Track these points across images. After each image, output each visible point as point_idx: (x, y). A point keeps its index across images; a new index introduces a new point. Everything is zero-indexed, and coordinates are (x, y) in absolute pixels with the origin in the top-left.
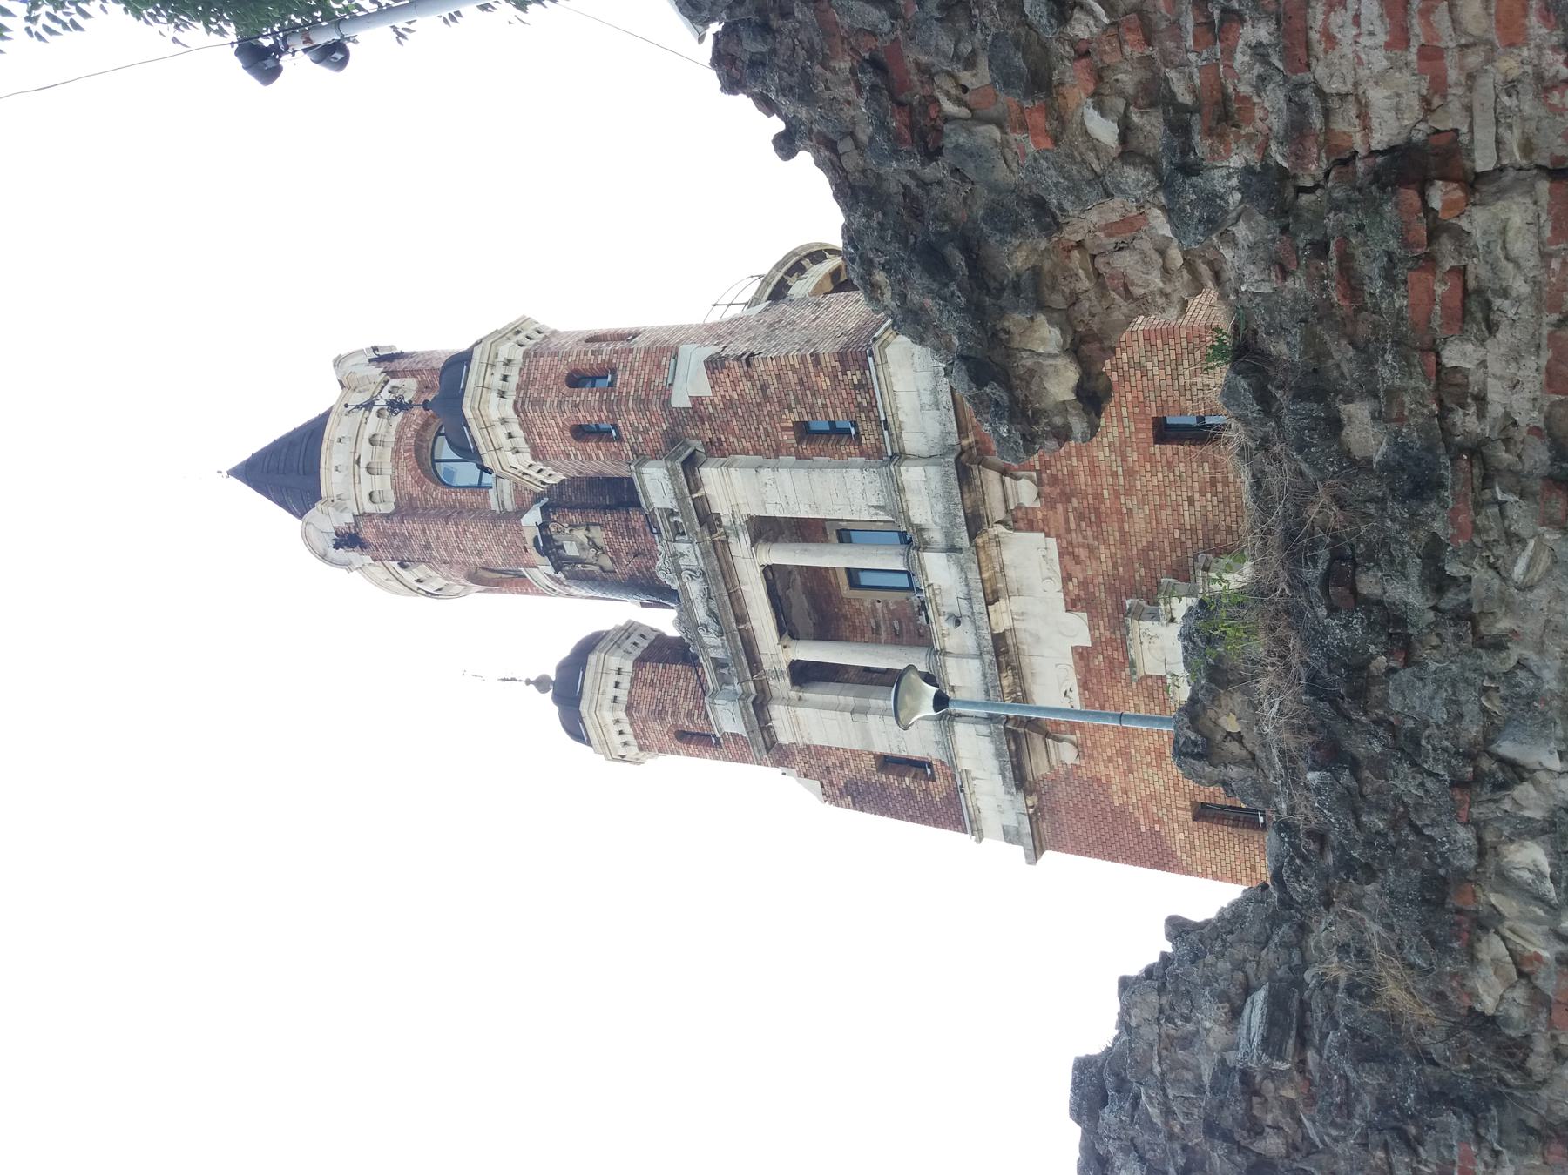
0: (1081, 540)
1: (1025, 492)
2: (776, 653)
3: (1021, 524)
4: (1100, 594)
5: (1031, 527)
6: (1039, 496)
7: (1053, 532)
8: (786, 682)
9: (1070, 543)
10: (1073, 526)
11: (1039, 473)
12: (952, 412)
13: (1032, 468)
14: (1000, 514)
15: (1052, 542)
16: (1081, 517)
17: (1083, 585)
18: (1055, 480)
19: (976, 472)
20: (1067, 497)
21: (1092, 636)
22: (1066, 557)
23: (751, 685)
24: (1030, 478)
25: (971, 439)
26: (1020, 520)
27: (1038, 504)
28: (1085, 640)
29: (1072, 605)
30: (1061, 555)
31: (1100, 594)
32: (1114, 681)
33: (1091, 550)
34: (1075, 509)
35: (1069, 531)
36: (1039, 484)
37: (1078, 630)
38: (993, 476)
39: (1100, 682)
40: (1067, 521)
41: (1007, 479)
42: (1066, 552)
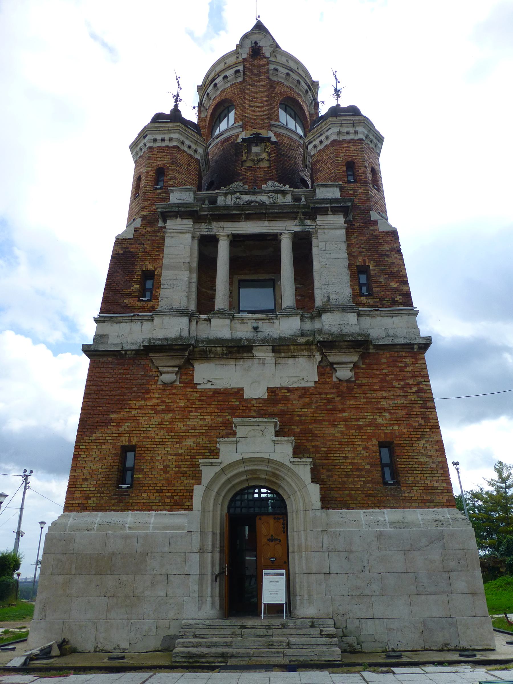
0: (314, 400)
1: (344, 373)
2: (225, 230)
3: (321, 370)
4: (281, 406)
5: (320, 374)
6: (340, 380)
7: (318, 385)
8: (204, 232)
9: (312, 394)
10: (323, 396)
11: (354, 382)
12: (390, 343)
13: (357, 379)
14: (331, 359)
15: (312, 385)
16: (329, 401)
17: (286, 398)
18: (350, 390)
19: (358, 350)
20: (340, 394)
21: (252, 399)
22: (303, 391)
23: (206, 213)
24: (351, 378)
25: (371, 351)
26: (326, 369)
27: (335, 379)
28: (248, 394)
29: (271, 390)
30: (304, 388)
31: (281, 406)
32: (222, 409)
33: (309, 404)
34: (334, 398)
35: (320, 394)
36: (348, 381)
37: (255, 392)
38: (355, 358)
39: (219, 401)
40: (326, 393)
41: (352, 366)
42: (305, 390)
